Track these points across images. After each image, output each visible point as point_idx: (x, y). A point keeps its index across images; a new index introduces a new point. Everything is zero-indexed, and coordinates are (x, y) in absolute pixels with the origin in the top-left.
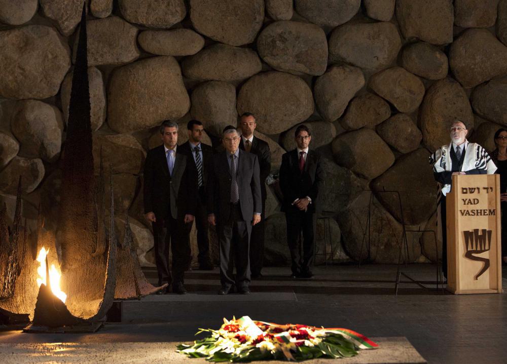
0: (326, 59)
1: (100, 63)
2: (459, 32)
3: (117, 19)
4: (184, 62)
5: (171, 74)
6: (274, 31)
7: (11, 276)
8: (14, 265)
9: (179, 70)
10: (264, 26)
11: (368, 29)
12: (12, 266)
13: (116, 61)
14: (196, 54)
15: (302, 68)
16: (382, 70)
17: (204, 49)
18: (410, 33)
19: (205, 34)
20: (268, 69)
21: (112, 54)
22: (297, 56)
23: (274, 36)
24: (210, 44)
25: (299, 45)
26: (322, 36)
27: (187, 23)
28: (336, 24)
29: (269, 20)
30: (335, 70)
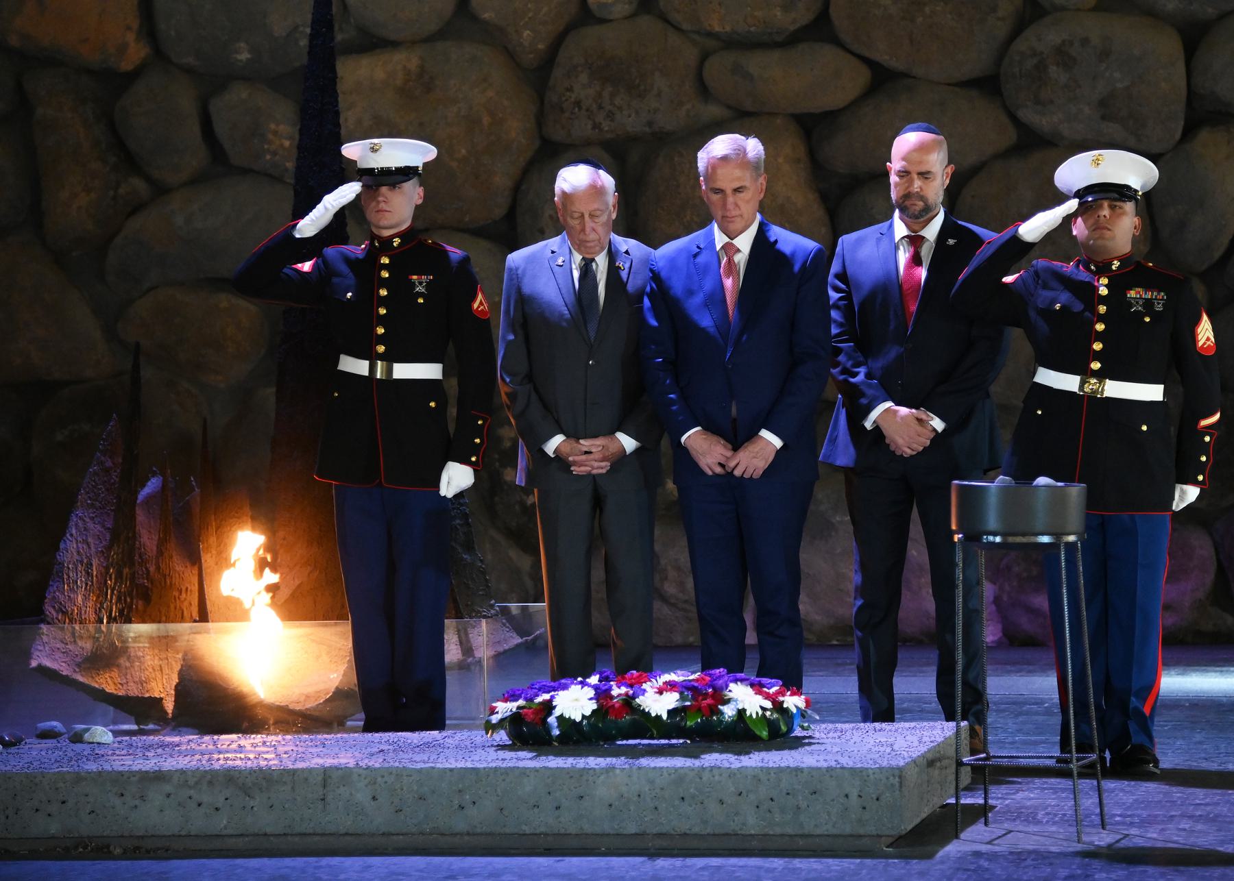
0: (1179, 109)
1: (609, 136)
3: (646, 23)
5: (780, 160)
7: (119, 599)
8: (126, 571)
9: (801, 151)
10: (1020, 26)
12: (119, 576)
13: (647, 129)
14: (844, 109)
19: (867, 54)
21: (637, 113)
22: (1103, 103)
23: (1042, 53)
25: (1107, 74)
26: (1168, 46)
27: (820, 29)
28: (1211, 11)
30: (1204, 135)
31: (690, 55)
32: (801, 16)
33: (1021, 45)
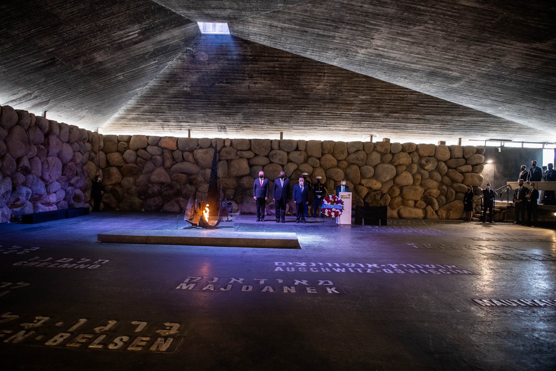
2: (323, 154)
3: (231, 148)
4: (248, 159)
6: (273, 152)
10: (271, 151)
11: (299, 152)
15: (280, 162)
16: (302, 163)
17: (255, 156)
18: (310, 154)
20: (271, 162)
24: (256, 155)
26: (286, 154)
27: (250, 149)
29: (272, 149)
30: (289, 163)
31: (236, 151)
32: (248, 148)
33: (272, 152)
